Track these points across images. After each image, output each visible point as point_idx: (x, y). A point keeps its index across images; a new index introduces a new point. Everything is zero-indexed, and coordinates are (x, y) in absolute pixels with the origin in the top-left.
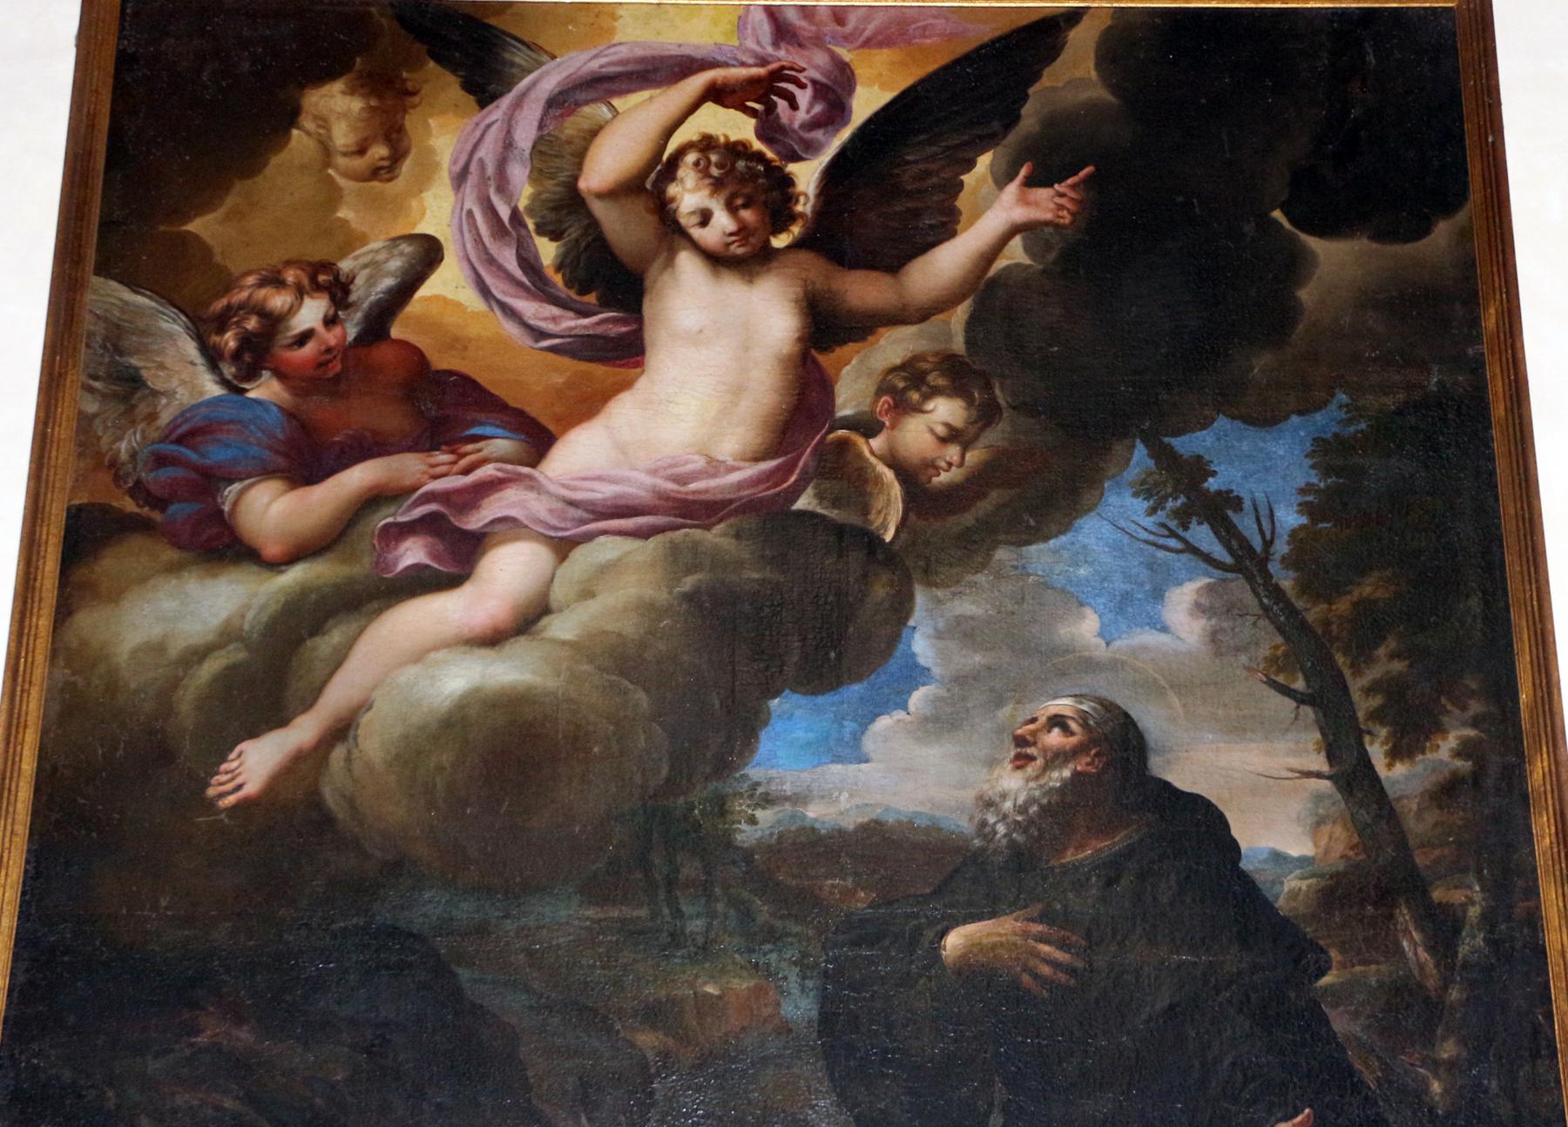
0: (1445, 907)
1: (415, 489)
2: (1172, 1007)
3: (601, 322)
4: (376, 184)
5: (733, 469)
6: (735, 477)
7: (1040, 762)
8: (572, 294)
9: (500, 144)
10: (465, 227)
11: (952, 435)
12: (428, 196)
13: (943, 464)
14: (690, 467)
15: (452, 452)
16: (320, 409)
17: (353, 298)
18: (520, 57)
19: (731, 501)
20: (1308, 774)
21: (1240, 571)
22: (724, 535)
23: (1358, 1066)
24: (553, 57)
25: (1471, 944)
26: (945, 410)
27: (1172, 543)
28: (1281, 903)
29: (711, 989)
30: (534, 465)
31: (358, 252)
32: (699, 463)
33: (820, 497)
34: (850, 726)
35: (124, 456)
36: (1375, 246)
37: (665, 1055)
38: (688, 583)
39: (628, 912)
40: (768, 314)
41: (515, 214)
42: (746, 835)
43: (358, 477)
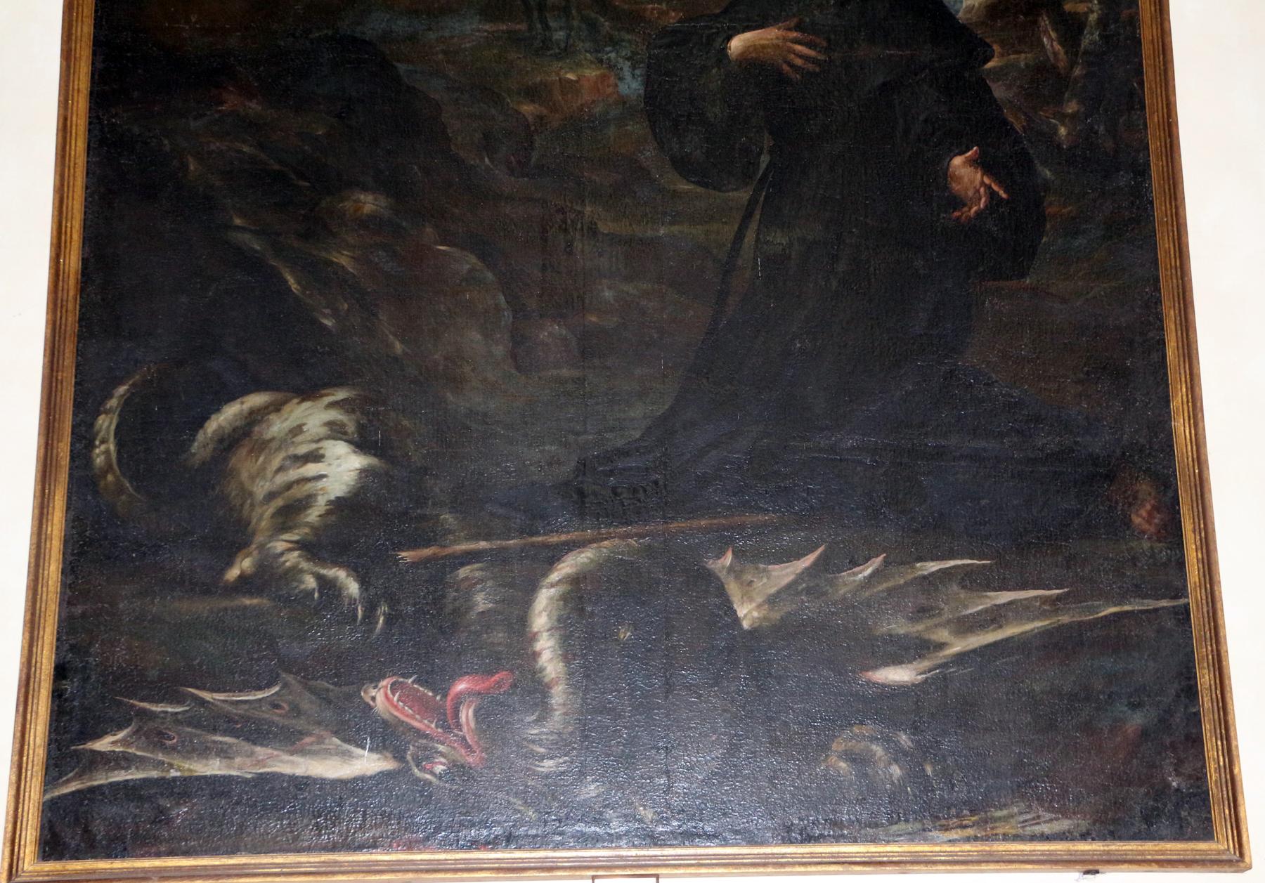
0: (1074, 15)
2: (884, 84)
23: (1011, 119)
25: (1090, 38)
28: (960, 15)
29: (571, 76)
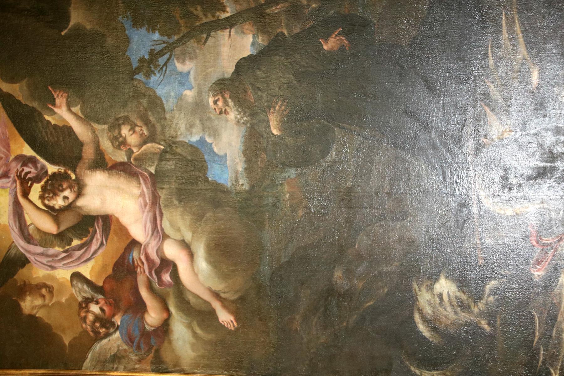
1: (148, 277)
2: (293, 75)
4: (54, 292)
6: (145, 190)
7: (227, 108)
8: (89, 235)
10: (69, 266)
11: (133, 129)
12: (58, 277)
14: (142, 202)
16: (123, 305)
17: (90, 297)
18: (13, 252)
20: (230, 35)
24: (13, 242)
26: (125, 131)
27: (164, 69)
28: (266, 44)
29: (287, 196)
30: (141, 245)
32: (141, 199)
33: (150, 166)
35: (137, 358)
36: (72, 5)
38: (176, 202)
40: (96, 181)
41: (64, 252)
42: (246, 187)
43: (144, 293)
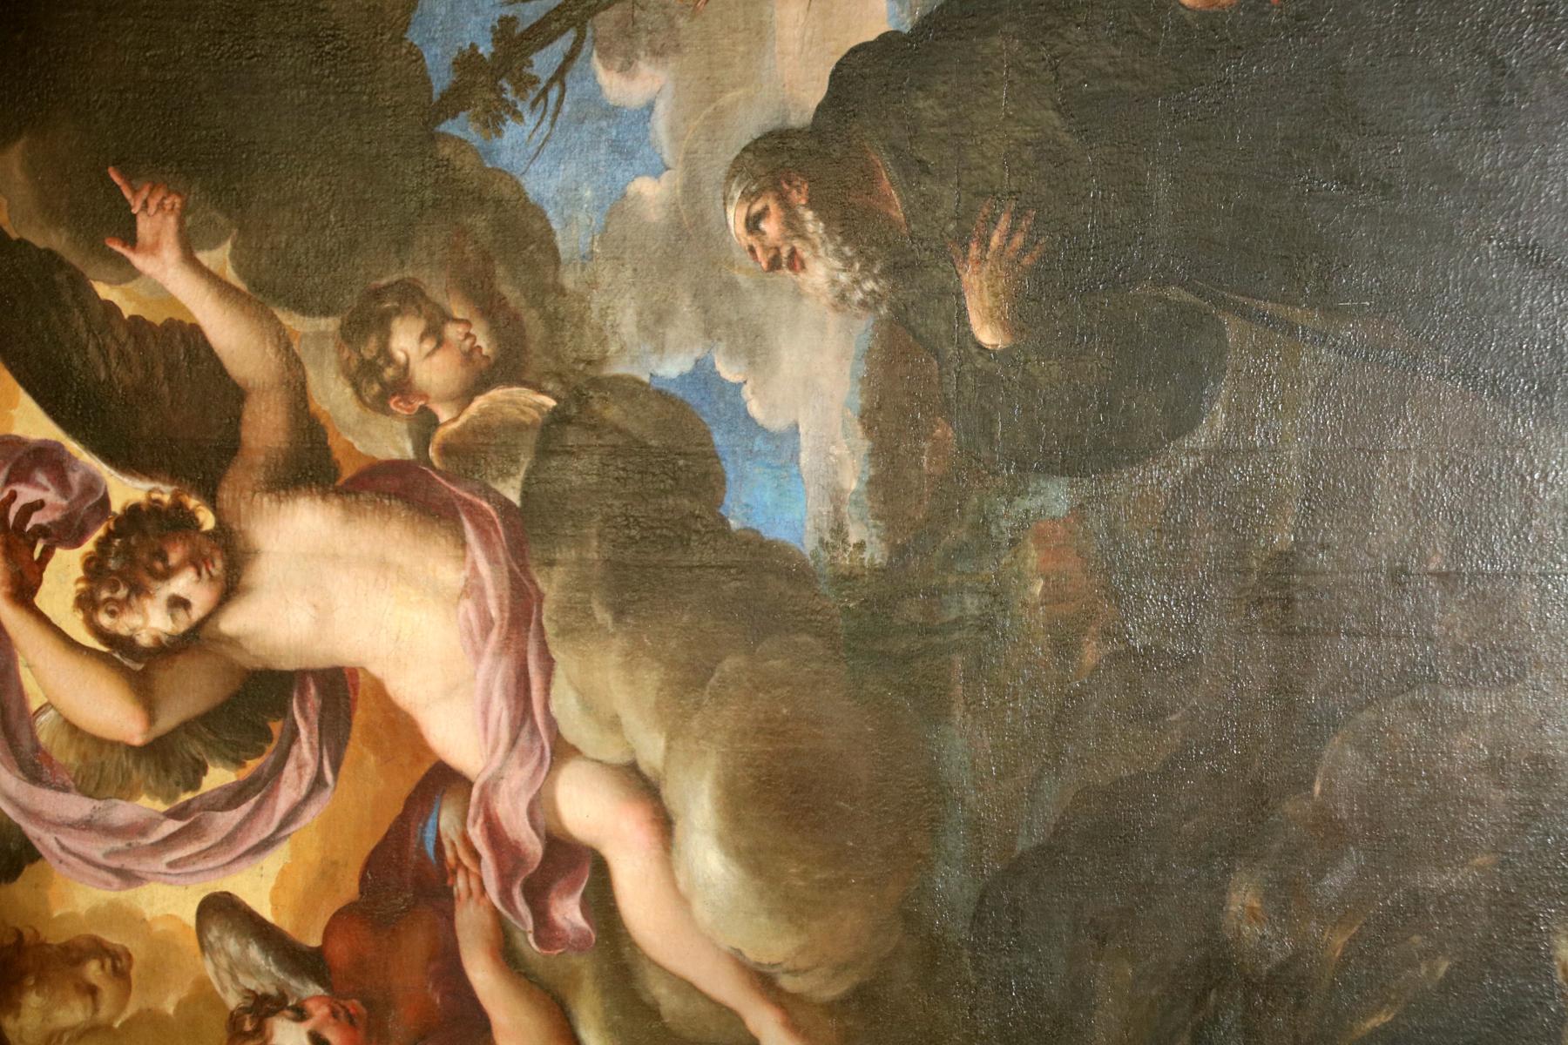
1: (496, 912)
2: (1057, 108)
3: (305, 720)
4: (133, 973)
5: (474, 568)
6: (484, 568)
7: (797, 243)
8: (271, 748)
9: (85, 834)
10: (190, 869)
11: (434, 334)
12: (149, 913)
13: (468, 342)
14: (473, 616)
15: (455, 873)
17: (272, 991)
19: (511, 571)
21: (584, 23)
22: (549, 580)
26: (405, 340)
27: (553, 95)
29: (1038, 588)
31: (218, 989)
32: (467, 605)
33: (505, 475)
34: (759, 443)
37: (1107, 634)
38: (603, 616)
39: (958, 674)
41: (171, 815)
42: (876, 553)
43: (482, 975)
